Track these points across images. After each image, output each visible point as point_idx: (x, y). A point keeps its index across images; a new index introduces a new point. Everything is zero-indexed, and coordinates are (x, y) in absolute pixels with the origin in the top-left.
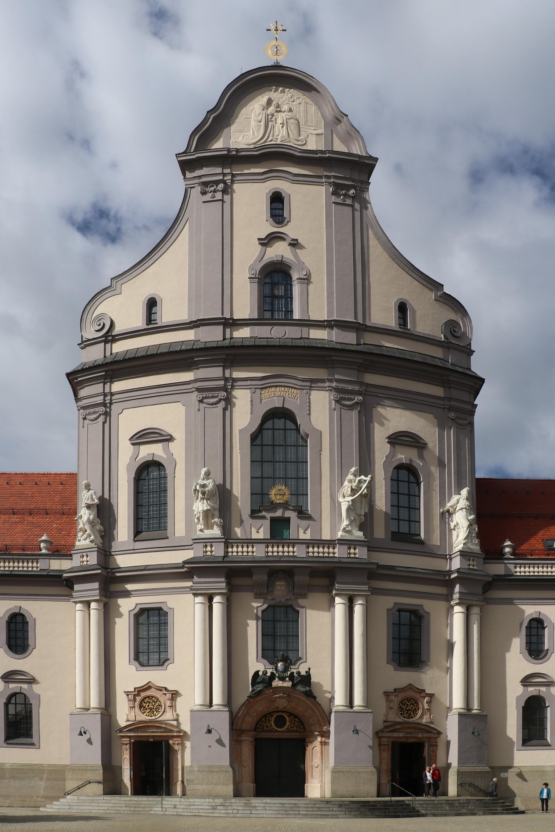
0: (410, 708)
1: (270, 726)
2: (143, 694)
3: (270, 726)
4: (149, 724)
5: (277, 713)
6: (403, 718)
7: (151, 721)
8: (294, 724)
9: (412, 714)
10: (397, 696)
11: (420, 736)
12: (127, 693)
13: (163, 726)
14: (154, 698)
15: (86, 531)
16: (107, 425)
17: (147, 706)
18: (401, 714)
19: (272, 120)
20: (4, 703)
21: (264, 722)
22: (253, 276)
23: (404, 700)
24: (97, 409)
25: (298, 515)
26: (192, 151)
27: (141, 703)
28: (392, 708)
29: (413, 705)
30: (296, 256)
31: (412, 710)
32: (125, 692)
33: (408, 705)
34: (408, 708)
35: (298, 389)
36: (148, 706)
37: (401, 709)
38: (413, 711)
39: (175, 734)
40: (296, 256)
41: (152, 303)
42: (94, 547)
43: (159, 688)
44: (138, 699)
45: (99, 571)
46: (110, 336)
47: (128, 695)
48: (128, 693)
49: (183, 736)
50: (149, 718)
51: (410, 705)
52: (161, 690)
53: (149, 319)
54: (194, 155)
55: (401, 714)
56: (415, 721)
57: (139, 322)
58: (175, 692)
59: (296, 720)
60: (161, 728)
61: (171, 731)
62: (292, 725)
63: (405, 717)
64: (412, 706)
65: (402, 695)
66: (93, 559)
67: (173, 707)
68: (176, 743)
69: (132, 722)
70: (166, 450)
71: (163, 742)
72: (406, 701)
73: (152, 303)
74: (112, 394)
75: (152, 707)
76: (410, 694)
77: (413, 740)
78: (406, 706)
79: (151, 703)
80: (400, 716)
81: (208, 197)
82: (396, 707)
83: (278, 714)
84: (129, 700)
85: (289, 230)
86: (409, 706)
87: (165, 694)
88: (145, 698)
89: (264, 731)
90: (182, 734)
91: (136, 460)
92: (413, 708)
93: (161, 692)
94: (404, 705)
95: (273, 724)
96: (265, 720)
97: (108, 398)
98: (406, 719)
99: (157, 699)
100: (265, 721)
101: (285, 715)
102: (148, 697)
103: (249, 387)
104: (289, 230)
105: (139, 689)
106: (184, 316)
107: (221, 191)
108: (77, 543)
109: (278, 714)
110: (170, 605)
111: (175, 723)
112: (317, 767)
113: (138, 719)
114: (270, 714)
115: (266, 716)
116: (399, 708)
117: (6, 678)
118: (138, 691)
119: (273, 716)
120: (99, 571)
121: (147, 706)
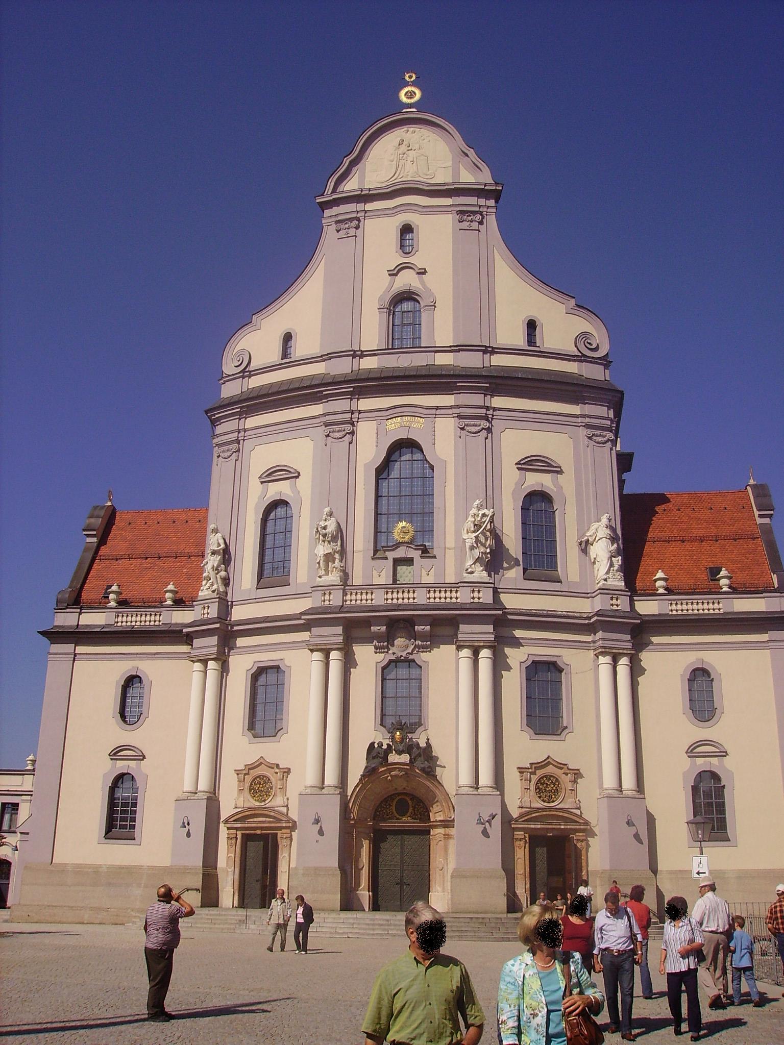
0: (550, 788)
1: (391, 813)
2: (254, 773)
3: (391, 813)
4: (256, 812)
5: (399, 796)
6: (542, 803)
7: (259, 808)
8: (418, 810)
9: (553, 796)
10: (534, 773)
11: (562, 827)
12: (238, 772)
13: (272, 814)
14: (265, 778)
15: (210, 579)
16: (239, 463)
17: (257, 788)
18: (539, 797)
19: (403, 158)
20: (110, 786)
21: (384, 807)
22: (382, 307)
23: (542, 778)
24: (231, 447)
25: (422, 553)
26: (329, 193)
27: (251, 784)
28: (528, 789)
29: (554, 784)
30: (423, 283)
31: (553, 791)
32: (235, 770)
33: (547, 784)
34: (547, 789)
35: (423, 418)
36: (259, 788)
37: (538, 790)
38: (554, 792)
39: (284, 825)
40: (423, 283)
41: (288, 338)
42: (216, 596)
43: (270, 766)
44: (249, 779)
45: (218, 625)
46: (247, 372)
47: (238, 774)
48: (238, 772)
49: (293, 827)
50: (258, 804)
51: (550, 785)
52: (273, 768)
53: (285, 354)
54: (331, 196)
55: (540, 797)
56: (557, 807)
57: (275, 357)
58: (286, 770)
59: (420, 805)
60: (270, 817)
61: (279, 820)
62: (416, 812)
63: (544, 801)
64: (552, 786)
65: (540, 773)
66: (213, 611)
67: (283, 789)
68: (285, 837)
69: (240, 809)
70: (294, 488)
71: (270, 836)
72: (545, 779)
73: (288, 338)
74: (245, 430)
75: (262, 789)
76: (550, 770)
77: (556, 833)
78: (545, 785)
79: (262, 784)
80: (538, 799)
81: (342, 234)
82: (533, 788)
83: (400, 797)
84: (239, 781)
85: (417, 260)
86: (549, 786)
87: (276, 773)
88: (255, 779)
89: (384, 820)
90: (291, 825)
91: (265, 499)
92: (555, 788)
93: (273, 770)
94: (542, 784)
95: (394, 811)
96: (385, 805)
97: (242, 434)
98: (546, 804)
99: (269, 779)
100: (385, 806)
101: (408, 799)
102: (259, 777)
103: (376, 418)
104: (417, 260)
105: (250, 767)
106: (316, 351)
107: (354, 228)
108: (200, 594)
109: (400, 797)
110: (287, 663)
111: (284, 810)
112: (441, 870)
113: (247, 805)
114: (391, 797)
115: (388, 800)
116: (536, 789)
117: (115, 754)
118: (249, 769)
119: (394, 800)
120: (218, 625)
121: (257, 788)
